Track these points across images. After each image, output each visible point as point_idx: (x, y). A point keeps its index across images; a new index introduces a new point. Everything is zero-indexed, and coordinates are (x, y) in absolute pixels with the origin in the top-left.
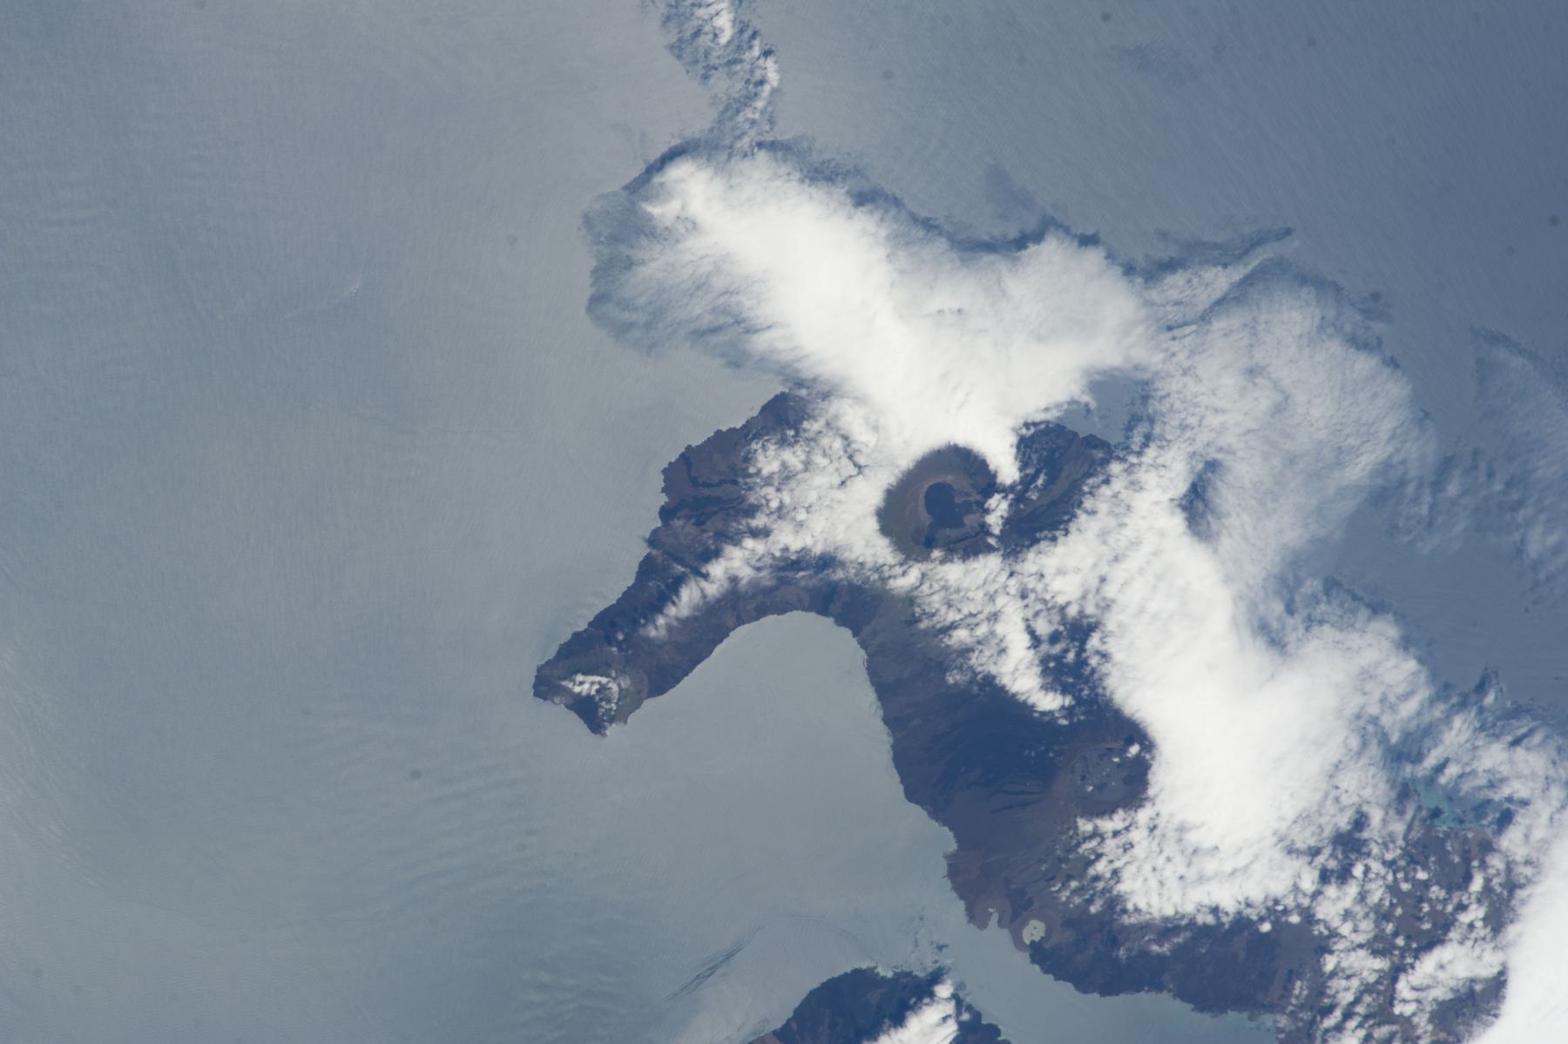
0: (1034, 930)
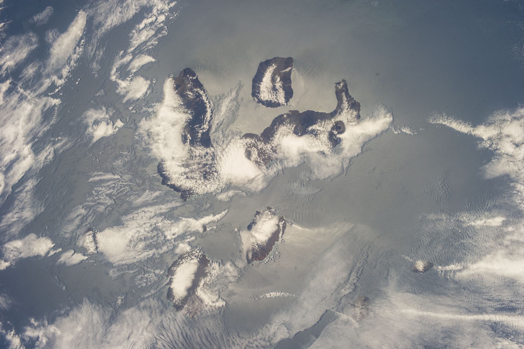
0: (285, 116)
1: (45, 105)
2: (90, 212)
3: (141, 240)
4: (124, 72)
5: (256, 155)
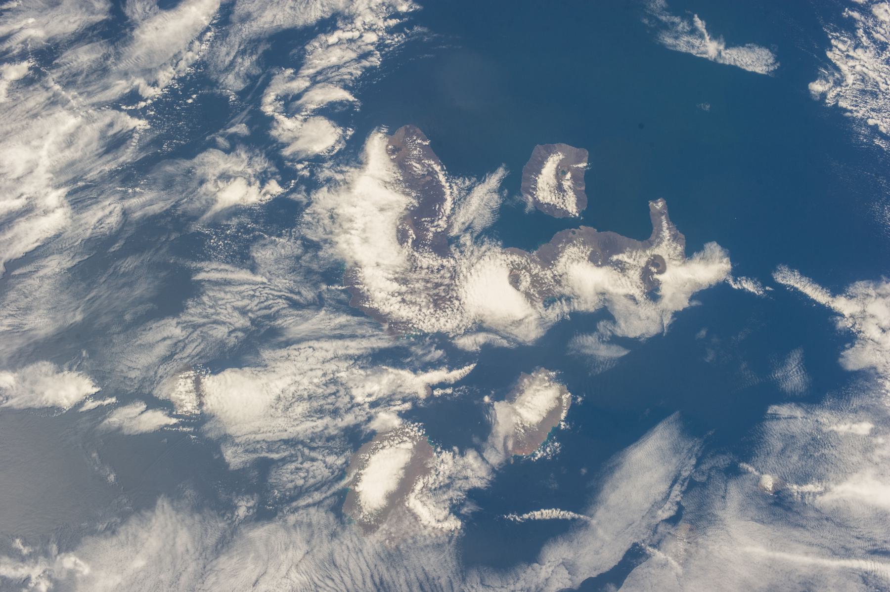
1: (111, 125)
2: (195, 335)
4: (290, 104)
5: (528, 283)
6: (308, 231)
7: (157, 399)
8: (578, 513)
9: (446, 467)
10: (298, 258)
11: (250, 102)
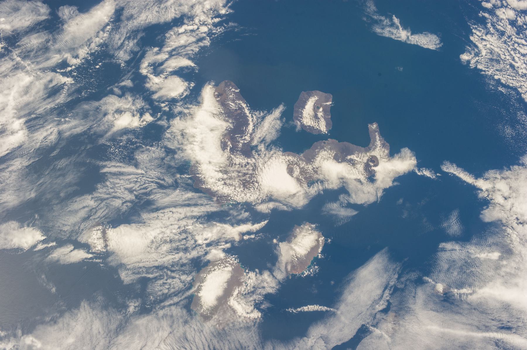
1: (51, 81)
2: (102, 205)
3: (165, 242)
4: (157, 68)
6: (169, 143)
7: (80, 242)
8: (330, 307)
9: (252, 281)
10: (163, 159)
11: (133, 67)
